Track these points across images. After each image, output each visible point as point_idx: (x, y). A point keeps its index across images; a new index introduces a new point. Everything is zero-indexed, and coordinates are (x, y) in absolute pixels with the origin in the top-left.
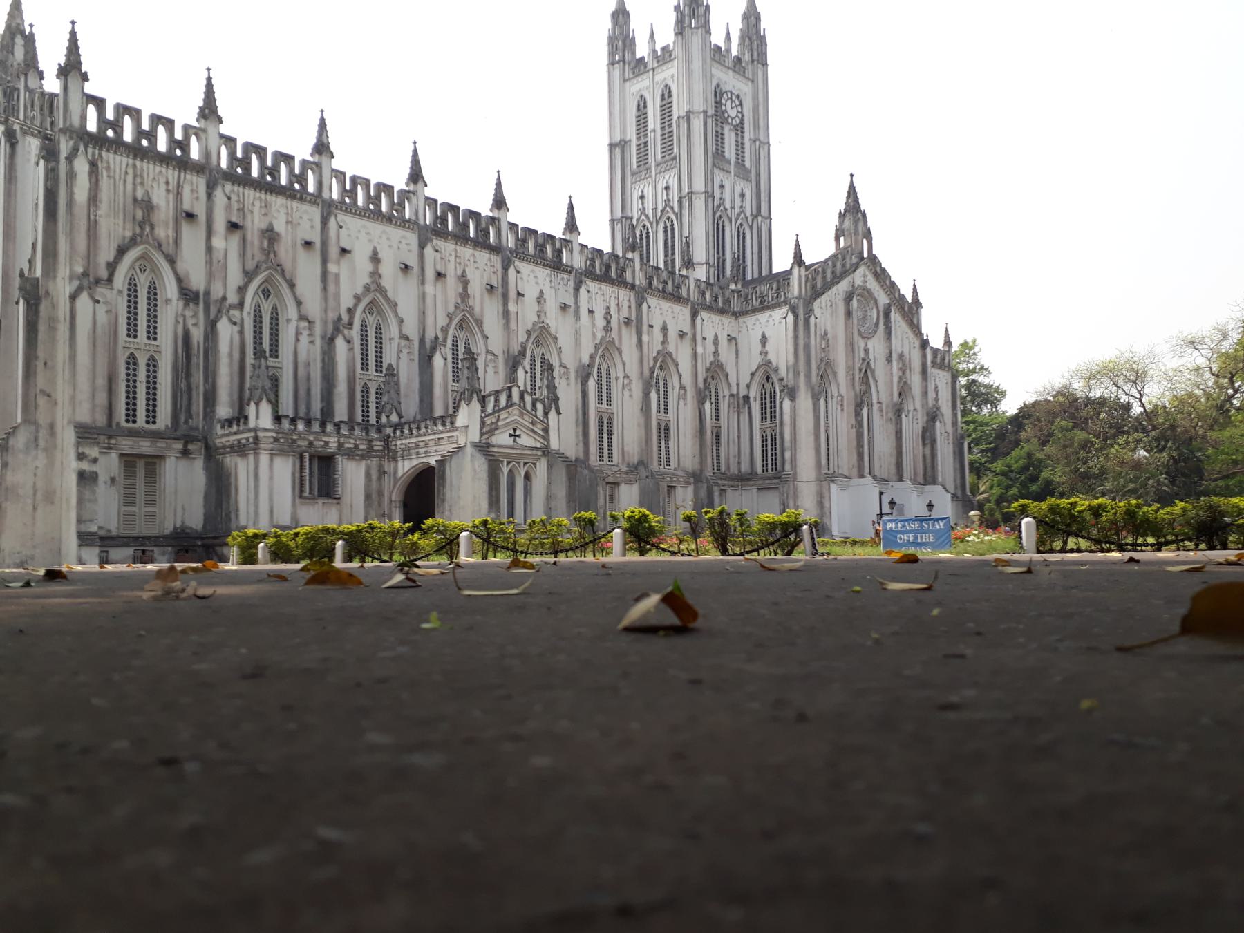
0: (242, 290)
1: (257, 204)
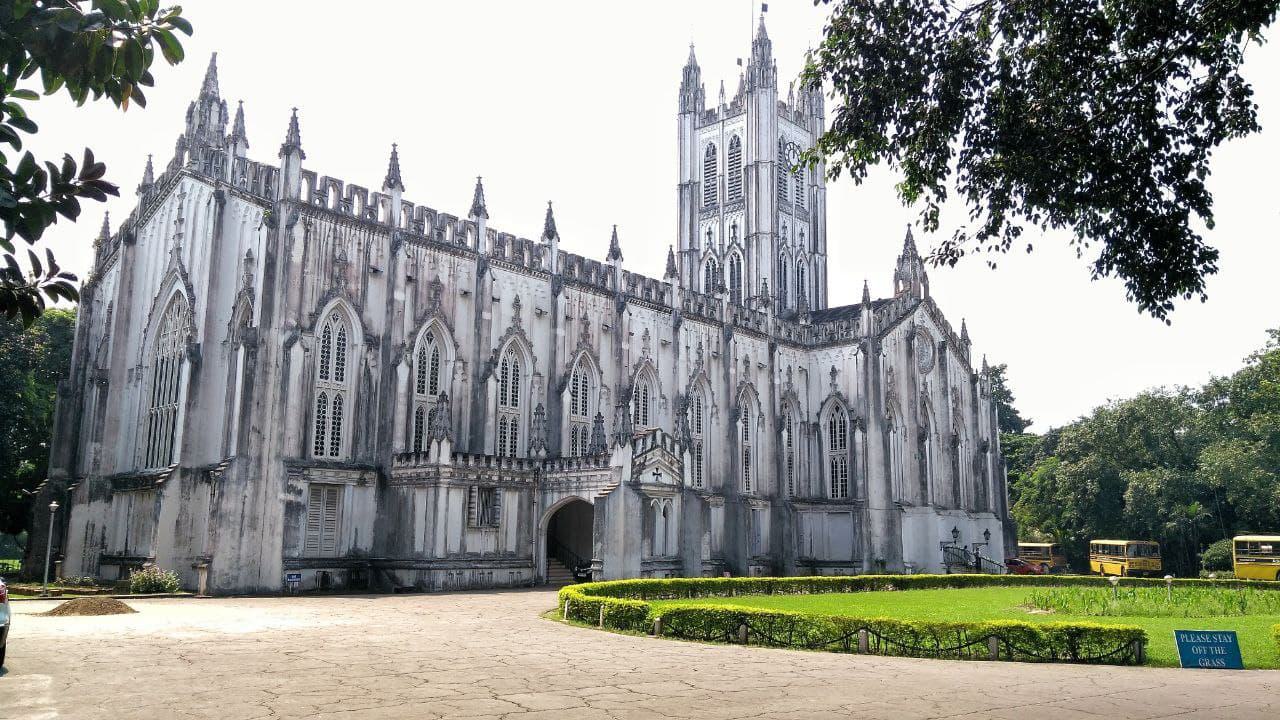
0: (413, 335)
1: (427, 260)
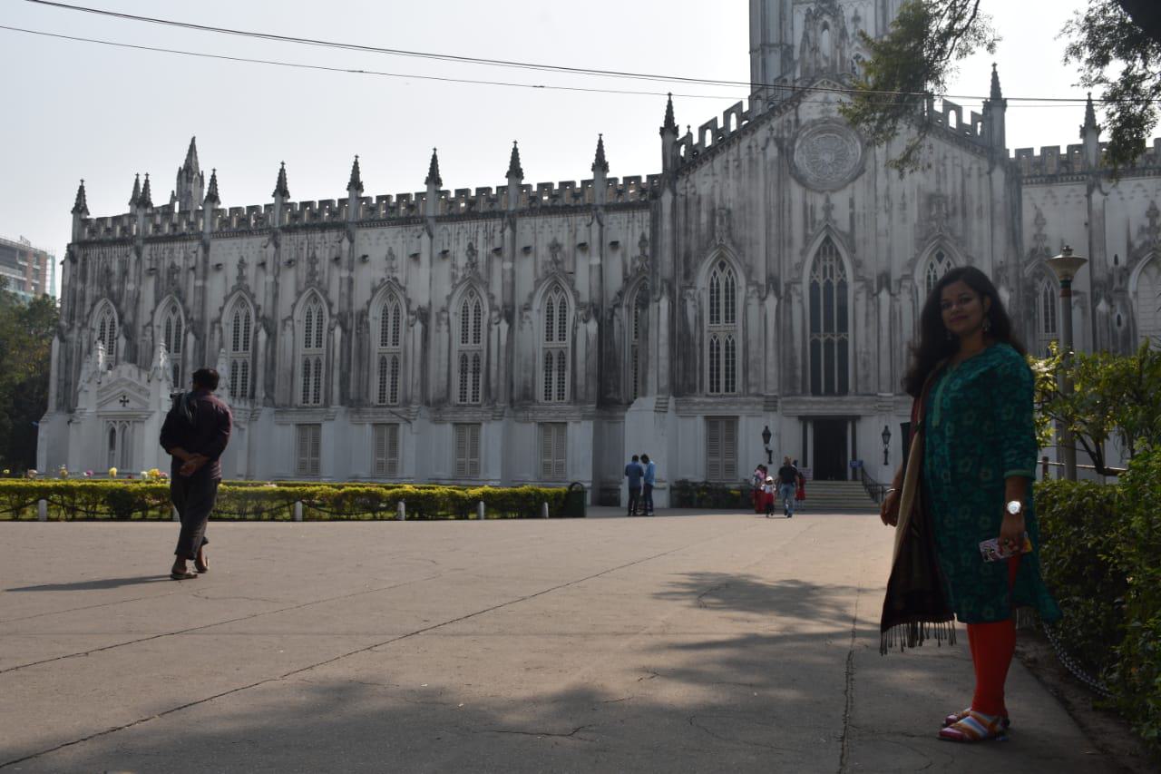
1: (167, 252)
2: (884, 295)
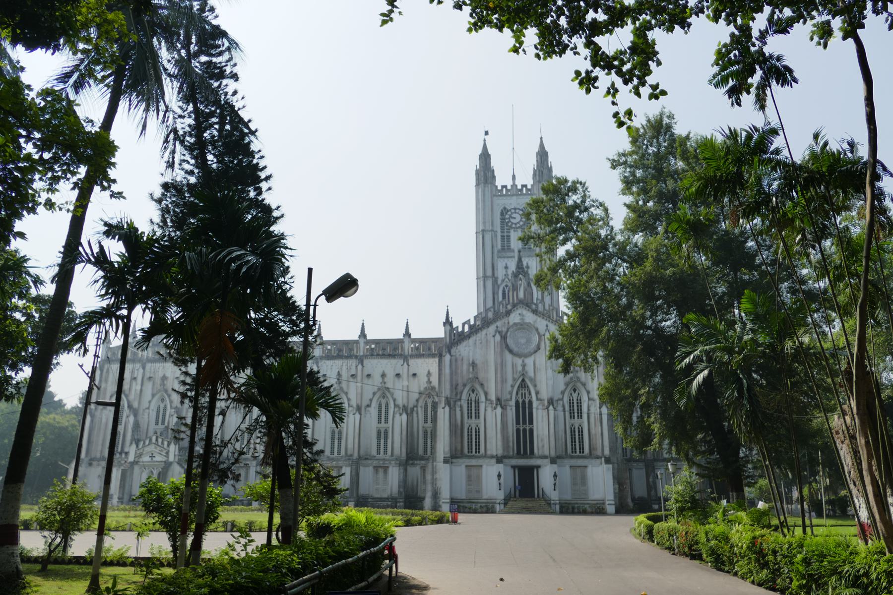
2: (551, 407)
